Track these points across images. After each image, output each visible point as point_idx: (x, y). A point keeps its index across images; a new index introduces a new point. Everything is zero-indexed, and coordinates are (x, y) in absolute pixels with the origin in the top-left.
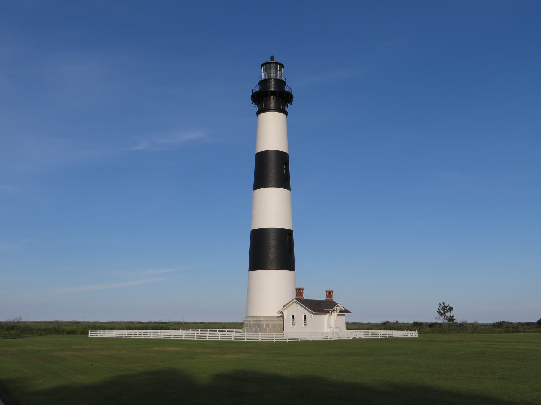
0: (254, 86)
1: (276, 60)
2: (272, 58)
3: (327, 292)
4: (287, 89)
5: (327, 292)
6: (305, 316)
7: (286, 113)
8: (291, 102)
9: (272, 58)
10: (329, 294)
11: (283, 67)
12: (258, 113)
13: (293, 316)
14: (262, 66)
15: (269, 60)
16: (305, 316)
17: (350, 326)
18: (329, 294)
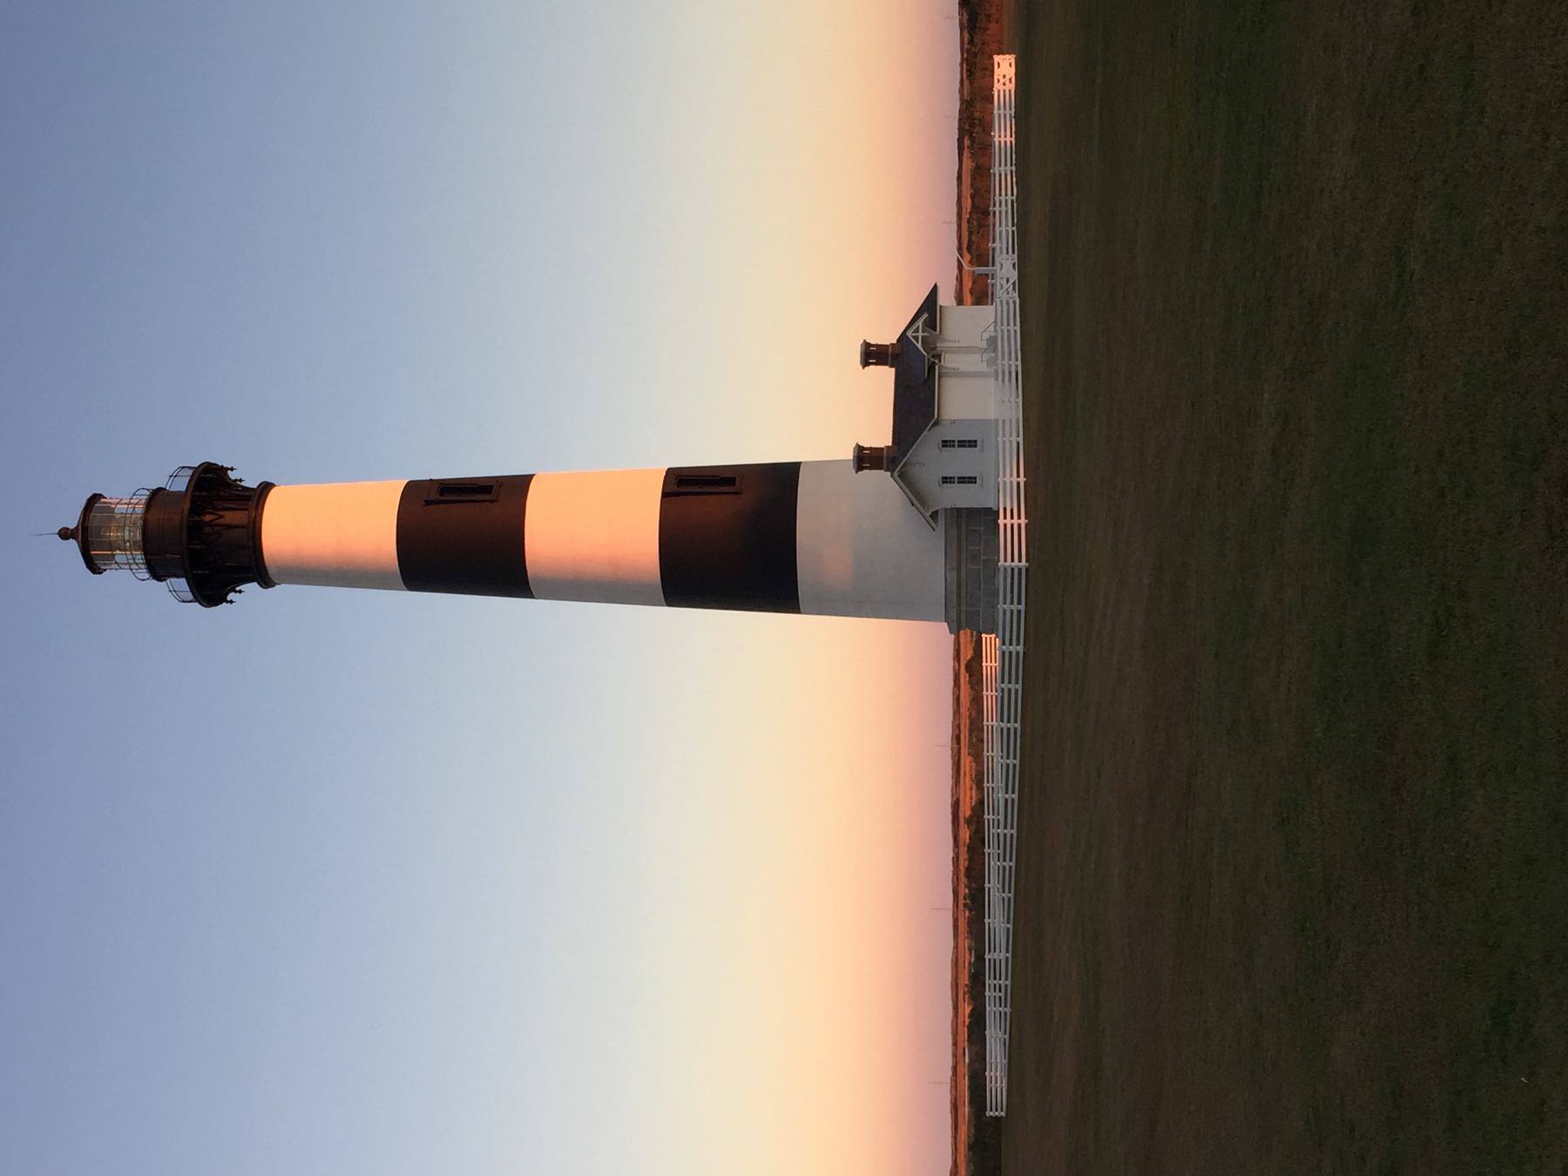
0: (166, 600)
1: (72, 523)
2: (65, 534)
3: (865, 363)
4: (181, 485)
5: (865, 363)
6: (946, 444)
7: (266, 487)
8: (223, 471)
9: (65, 534)
10: (872, 355)
11: (95, 498)
13: (946, 480)
14: (93, 567)
15: (73, 546)
16: (946, 444)
17: (980, 293)
18: (872, 355)
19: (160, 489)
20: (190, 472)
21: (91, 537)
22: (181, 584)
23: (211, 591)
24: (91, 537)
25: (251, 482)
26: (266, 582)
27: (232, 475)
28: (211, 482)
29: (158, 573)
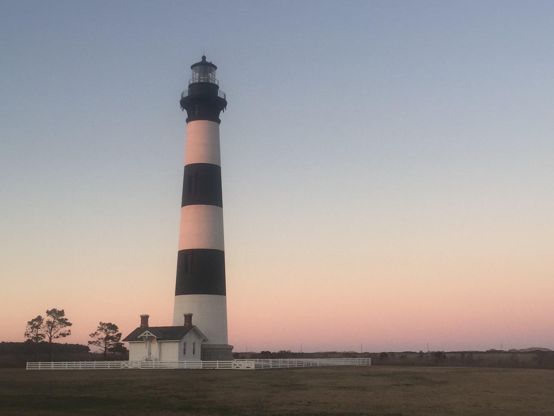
1: (208, 60)
2: (204, 58)
4: (220, 95)
9: (204, 58)
11: (215, 68)
12: (188, 121)
14: (193, 67)
15: (200, 60)
19: (218, 88)
20: (223, 98)
21: (205, 67)
22: (186, 95)
23: (185, 103)
24: (205, 67)
25: (221, 117)
26: (188, 121)
27: (222, 111)
28: (222, 104)
29: (191, 86)
